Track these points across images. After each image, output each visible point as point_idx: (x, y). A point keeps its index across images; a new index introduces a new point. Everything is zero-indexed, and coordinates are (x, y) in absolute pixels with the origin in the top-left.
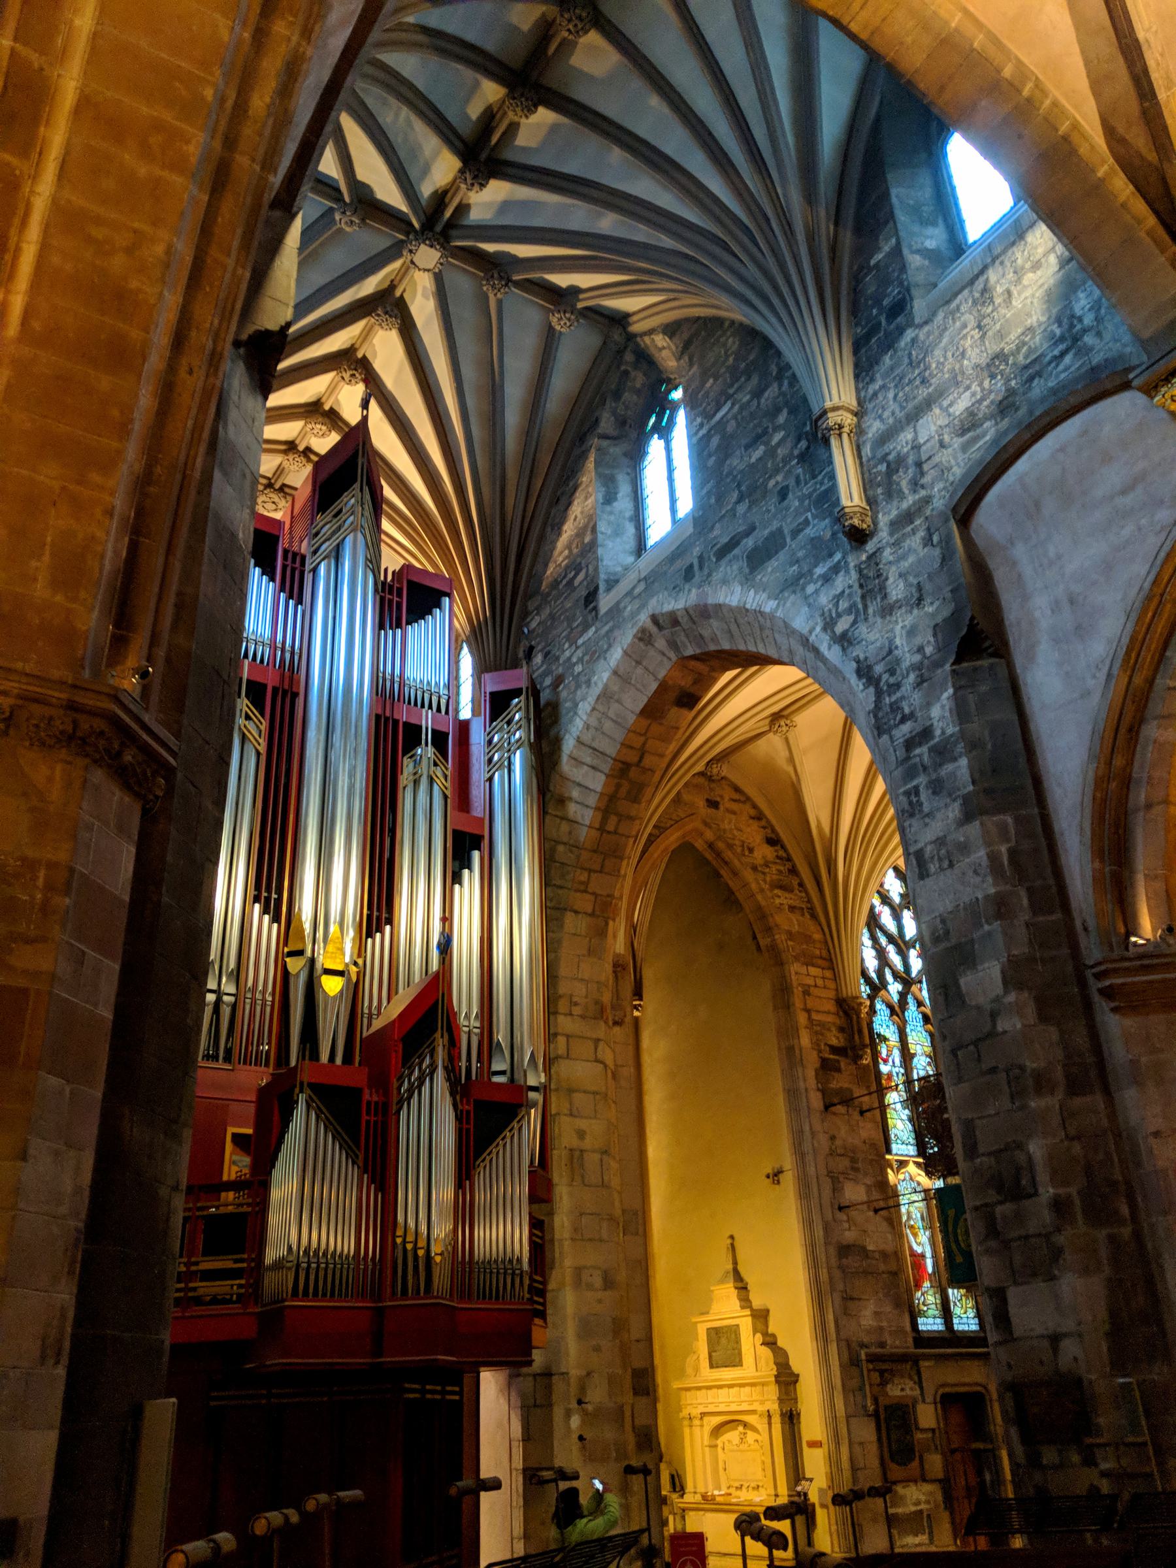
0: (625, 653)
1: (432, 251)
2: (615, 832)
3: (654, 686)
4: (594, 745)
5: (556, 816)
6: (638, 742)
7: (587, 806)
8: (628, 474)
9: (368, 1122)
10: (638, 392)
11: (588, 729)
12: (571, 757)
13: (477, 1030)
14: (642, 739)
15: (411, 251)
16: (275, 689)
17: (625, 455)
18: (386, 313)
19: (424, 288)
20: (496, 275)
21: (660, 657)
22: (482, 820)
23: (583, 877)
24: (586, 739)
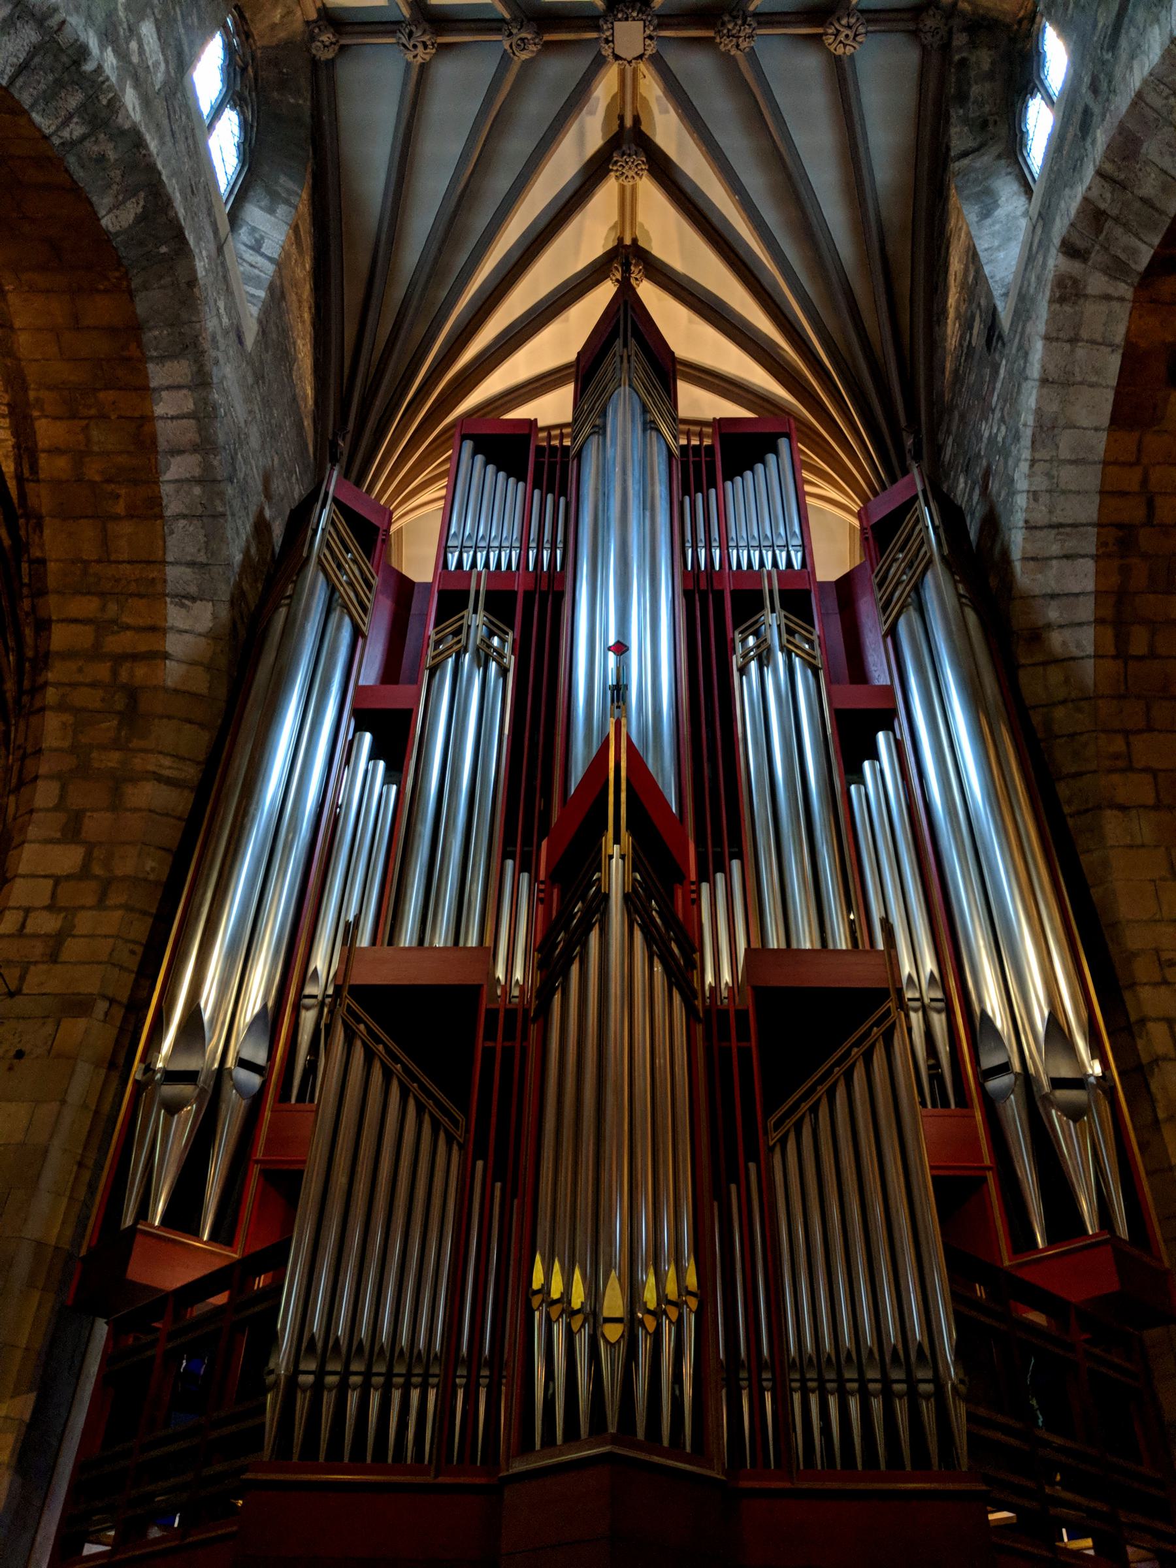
0: (1047, 338)
1: (629, 23)
2: (1153, 655)
3: (1114, 362)
4: (1055, 520)
5: (1034, 665)
6: (1131, 479)
7: (1080, 624)
8: (1010, 173)
9: (489, 1053)
10: (990, 76)
11: (1036, 500)
12: (1025, 559)
13: (940, 1005)
14: (1135, 475)
15: (607, 41)
16: (529, 596)
17: (999, 157)
18: (623, 154)
19: (658, 99)
20: (726, 18)
21: (1103, 307)
22: (889, 689)
23: (1118, 745)
24: (1041, 517)
